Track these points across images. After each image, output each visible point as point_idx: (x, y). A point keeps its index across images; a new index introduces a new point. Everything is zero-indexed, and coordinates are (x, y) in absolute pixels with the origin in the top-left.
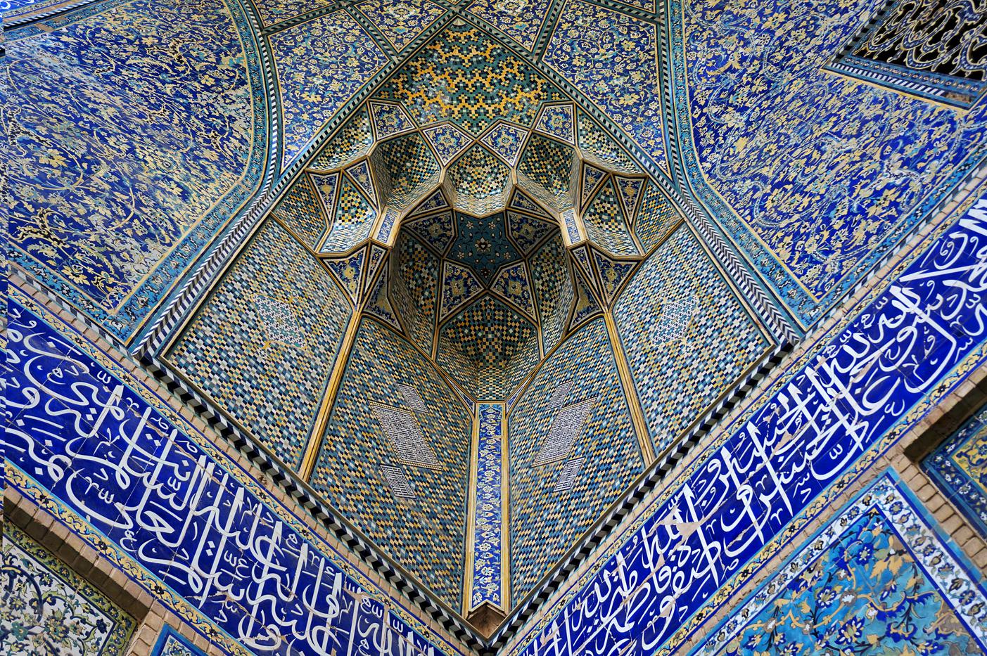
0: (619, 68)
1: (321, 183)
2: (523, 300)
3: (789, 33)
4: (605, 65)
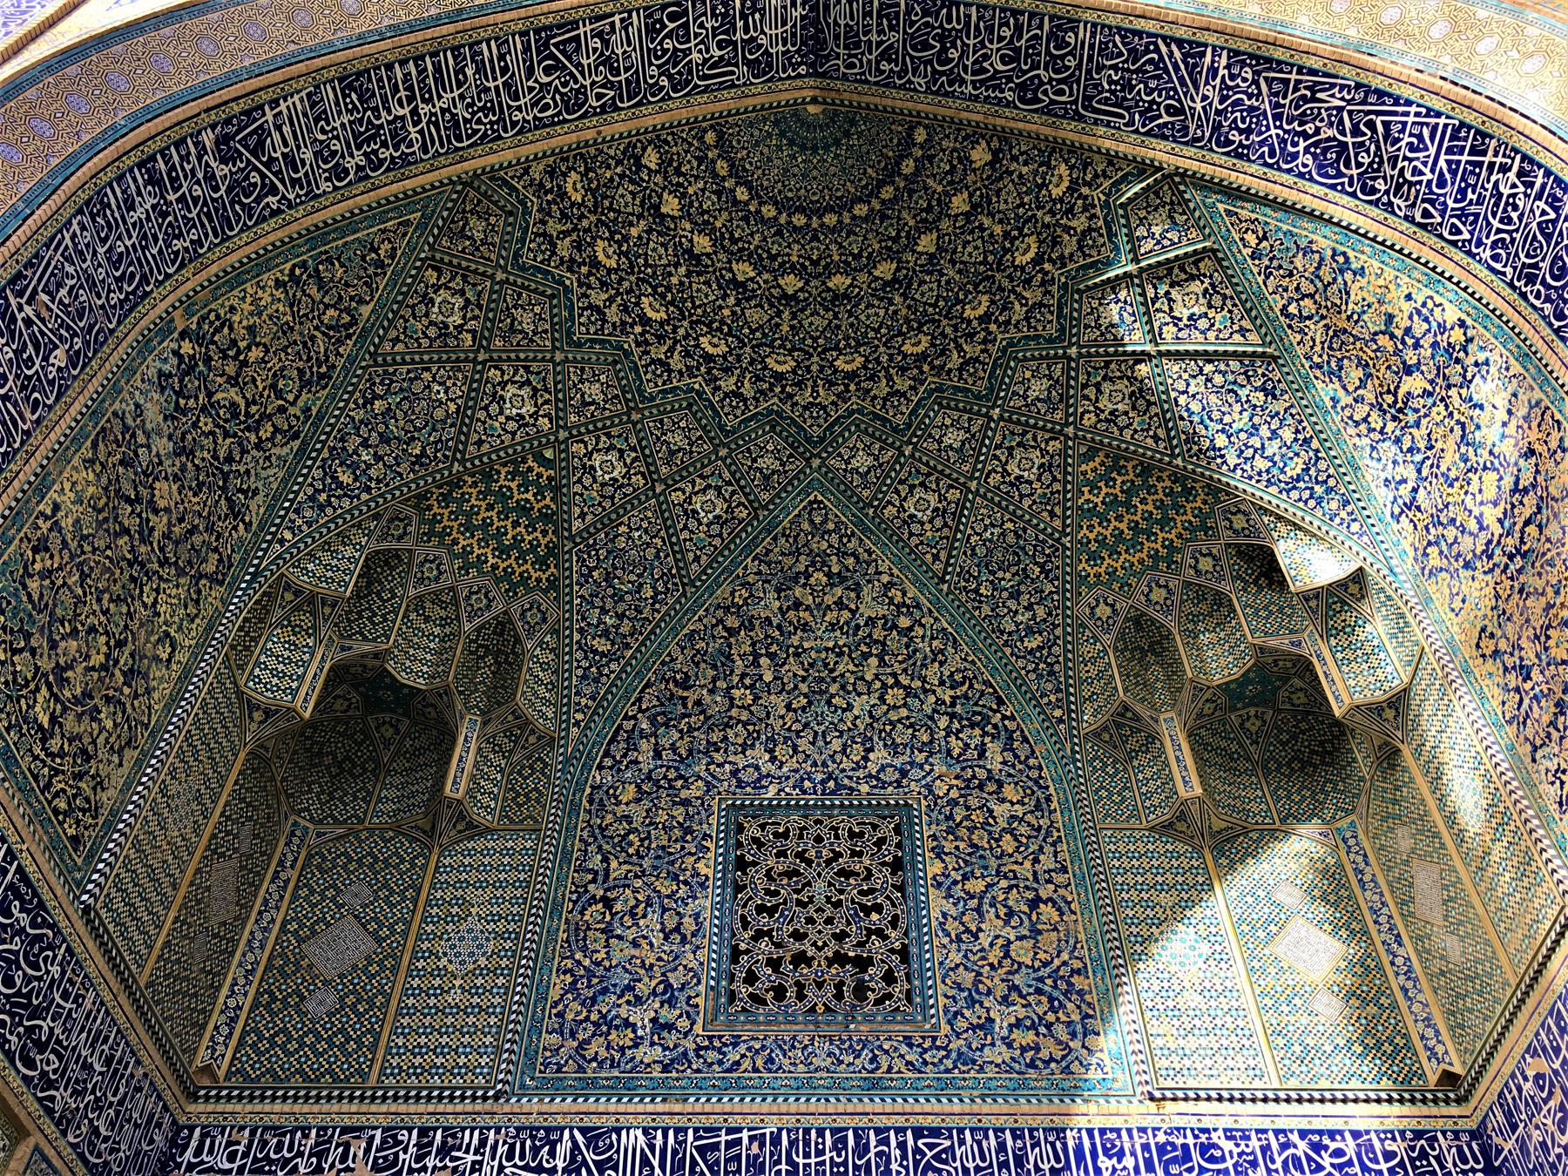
0: (620, 608)
2: (387, 743)
4: (615, 595)
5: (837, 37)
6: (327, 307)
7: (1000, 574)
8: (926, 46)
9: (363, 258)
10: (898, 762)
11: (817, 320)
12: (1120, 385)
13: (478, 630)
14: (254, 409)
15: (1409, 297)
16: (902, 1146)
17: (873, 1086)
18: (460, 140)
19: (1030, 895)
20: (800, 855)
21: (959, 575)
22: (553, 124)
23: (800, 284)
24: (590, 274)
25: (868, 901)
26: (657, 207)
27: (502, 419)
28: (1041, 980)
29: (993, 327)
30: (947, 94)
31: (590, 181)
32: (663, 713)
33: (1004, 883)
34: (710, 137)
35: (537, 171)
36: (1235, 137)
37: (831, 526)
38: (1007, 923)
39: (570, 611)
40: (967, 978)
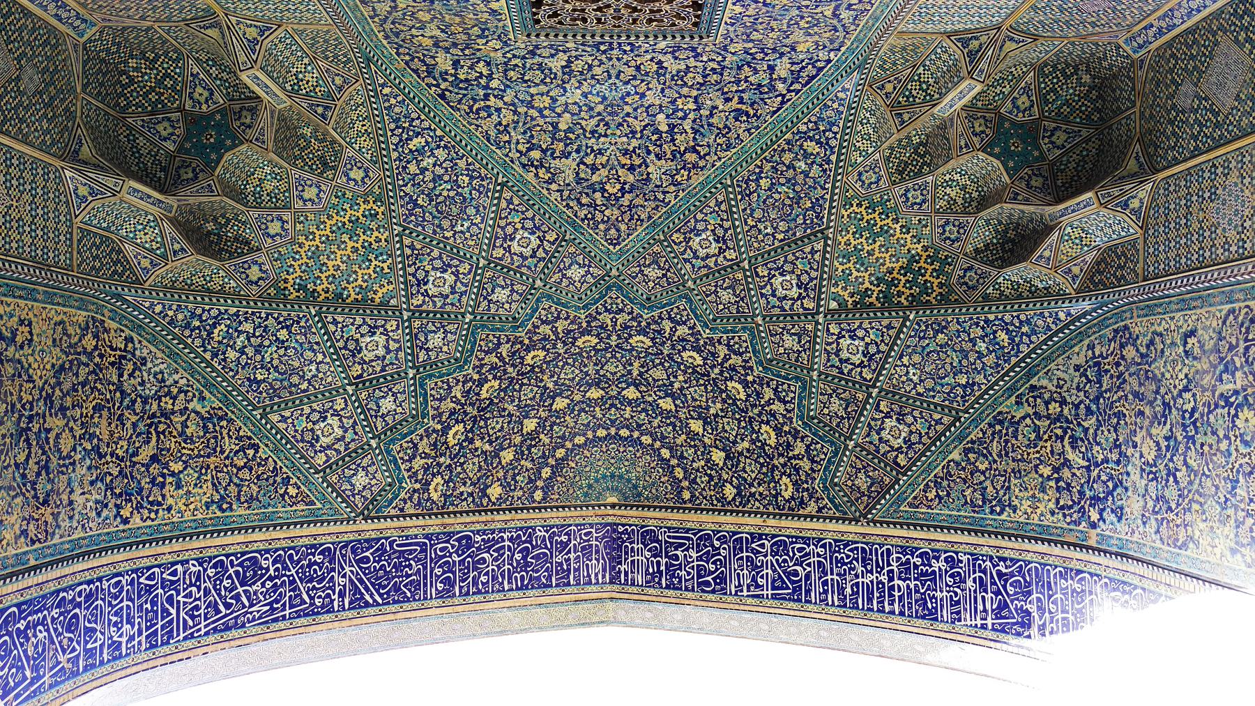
0: (791, 173)
1: (1074, 277)
2: (1026, 91)
3: (691, 87)
4: (794, 185)
5: (597, 552)
6: (983, 473)
7: (452, 194)
8: (537, 557)
9: (948, 495)
10: (537, 59)
11: (613, 370)
12: (370, 356)
14: (1059, 432)
15: (169, 509)
18: (863, 550)
21: (489, 190)
22: (797, 537)
26: (727, 457)
27: (867, 340)
29: (476, 377)
30: (521, 529)
32: (761, 93)
34: (686, 495)
35: (812, 508)
36: (318, 558)
37: (602, 226)
39: (835, 181)
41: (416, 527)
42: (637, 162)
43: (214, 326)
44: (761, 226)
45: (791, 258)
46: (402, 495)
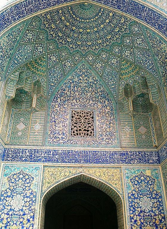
2: (23, 98)
7: (109, 77)
10: (93, 103)
12: (128, 51)
13: (35, 82)
16: (92, 153)
17: (88, 146)
18: (32, 12)
19: (110, 122)
20: (80, 116)
23: (82, 31)
24: (51, 29)
25: (89, 122)
28: (110, 133)
30: (107, 5)
31: (51, 15)
33: (106, 121)
34: (70, 8)
36: (148, 20)
38: (106, 126)
39: (48, 80)
40: (101, 133)
41: (128, 16)
42: (79, 81)
43: (151, 68)
44: (59, 69)
45: (53, 64)
46: (129, 22)
